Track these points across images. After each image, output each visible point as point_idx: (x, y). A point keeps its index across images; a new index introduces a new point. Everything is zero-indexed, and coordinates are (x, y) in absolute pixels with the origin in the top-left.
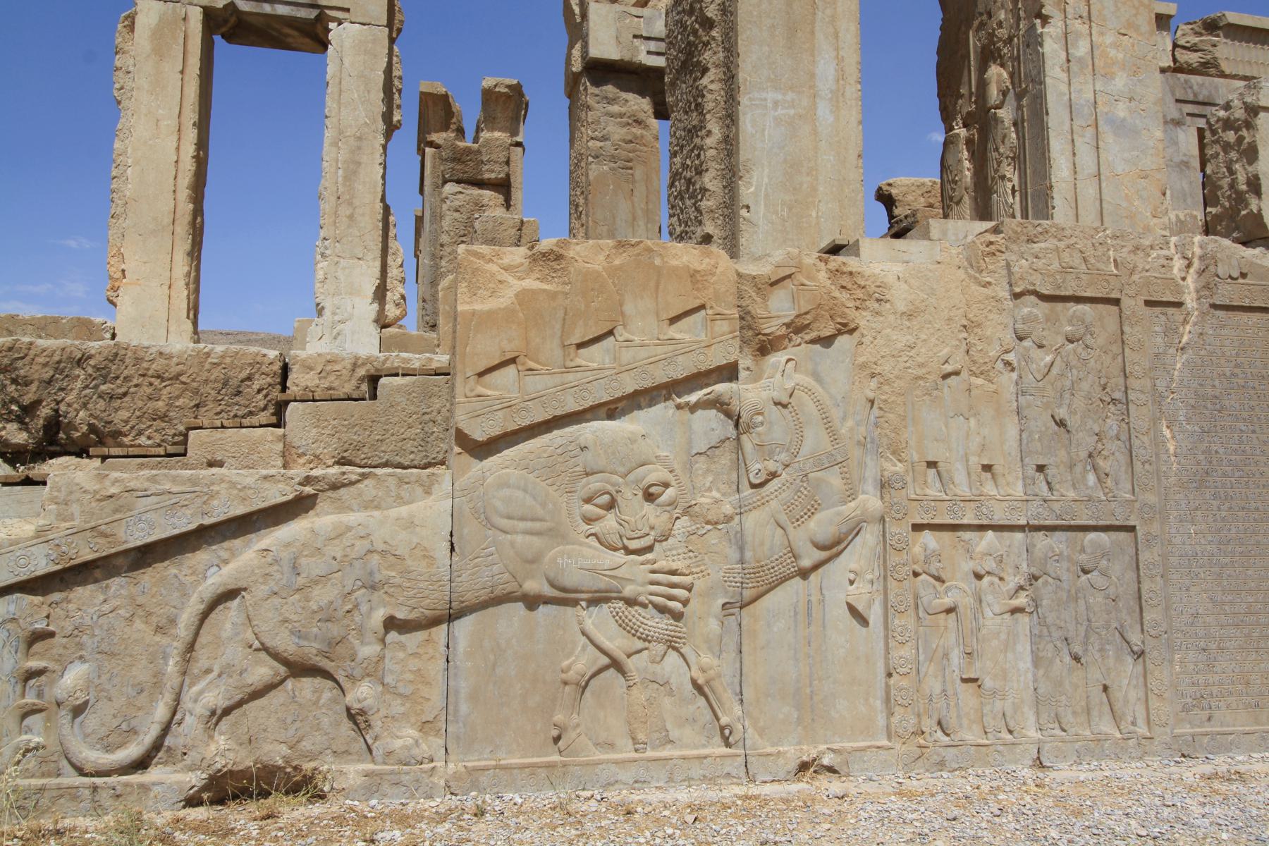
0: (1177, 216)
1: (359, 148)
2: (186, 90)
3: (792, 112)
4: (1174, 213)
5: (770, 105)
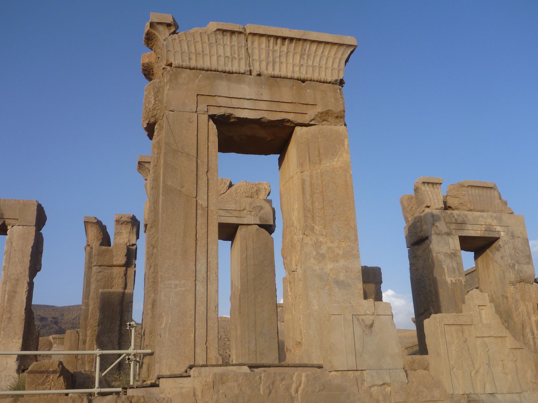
0: (451, 281)
3: (183, 289)
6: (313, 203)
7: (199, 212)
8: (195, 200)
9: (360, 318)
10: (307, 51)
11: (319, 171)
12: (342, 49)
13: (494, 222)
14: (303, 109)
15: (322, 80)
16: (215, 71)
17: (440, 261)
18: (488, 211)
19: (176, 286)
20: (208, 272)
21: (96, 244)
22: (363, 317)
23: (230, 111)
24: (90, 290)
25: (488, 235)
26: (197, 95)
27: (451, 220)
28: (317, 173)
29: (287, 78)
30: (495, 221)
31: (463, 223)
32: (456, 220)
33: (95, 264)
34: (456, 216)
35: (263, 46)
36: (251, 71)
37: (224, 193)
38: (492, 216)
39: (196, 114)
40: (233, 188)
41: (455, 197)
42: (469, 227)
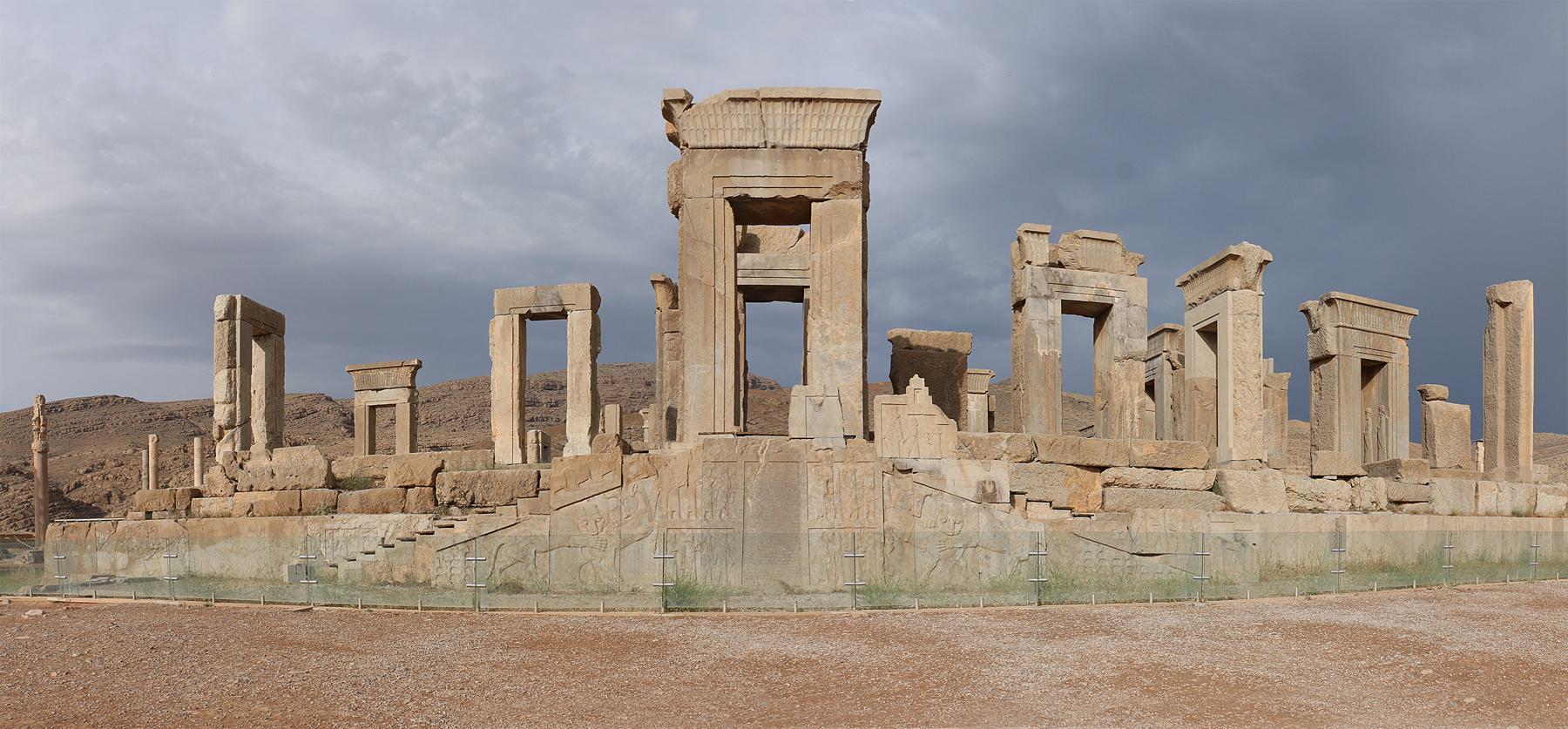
11: (829, 251)
16: (729, 148)
23: (745, 192)
28: (827, 253)
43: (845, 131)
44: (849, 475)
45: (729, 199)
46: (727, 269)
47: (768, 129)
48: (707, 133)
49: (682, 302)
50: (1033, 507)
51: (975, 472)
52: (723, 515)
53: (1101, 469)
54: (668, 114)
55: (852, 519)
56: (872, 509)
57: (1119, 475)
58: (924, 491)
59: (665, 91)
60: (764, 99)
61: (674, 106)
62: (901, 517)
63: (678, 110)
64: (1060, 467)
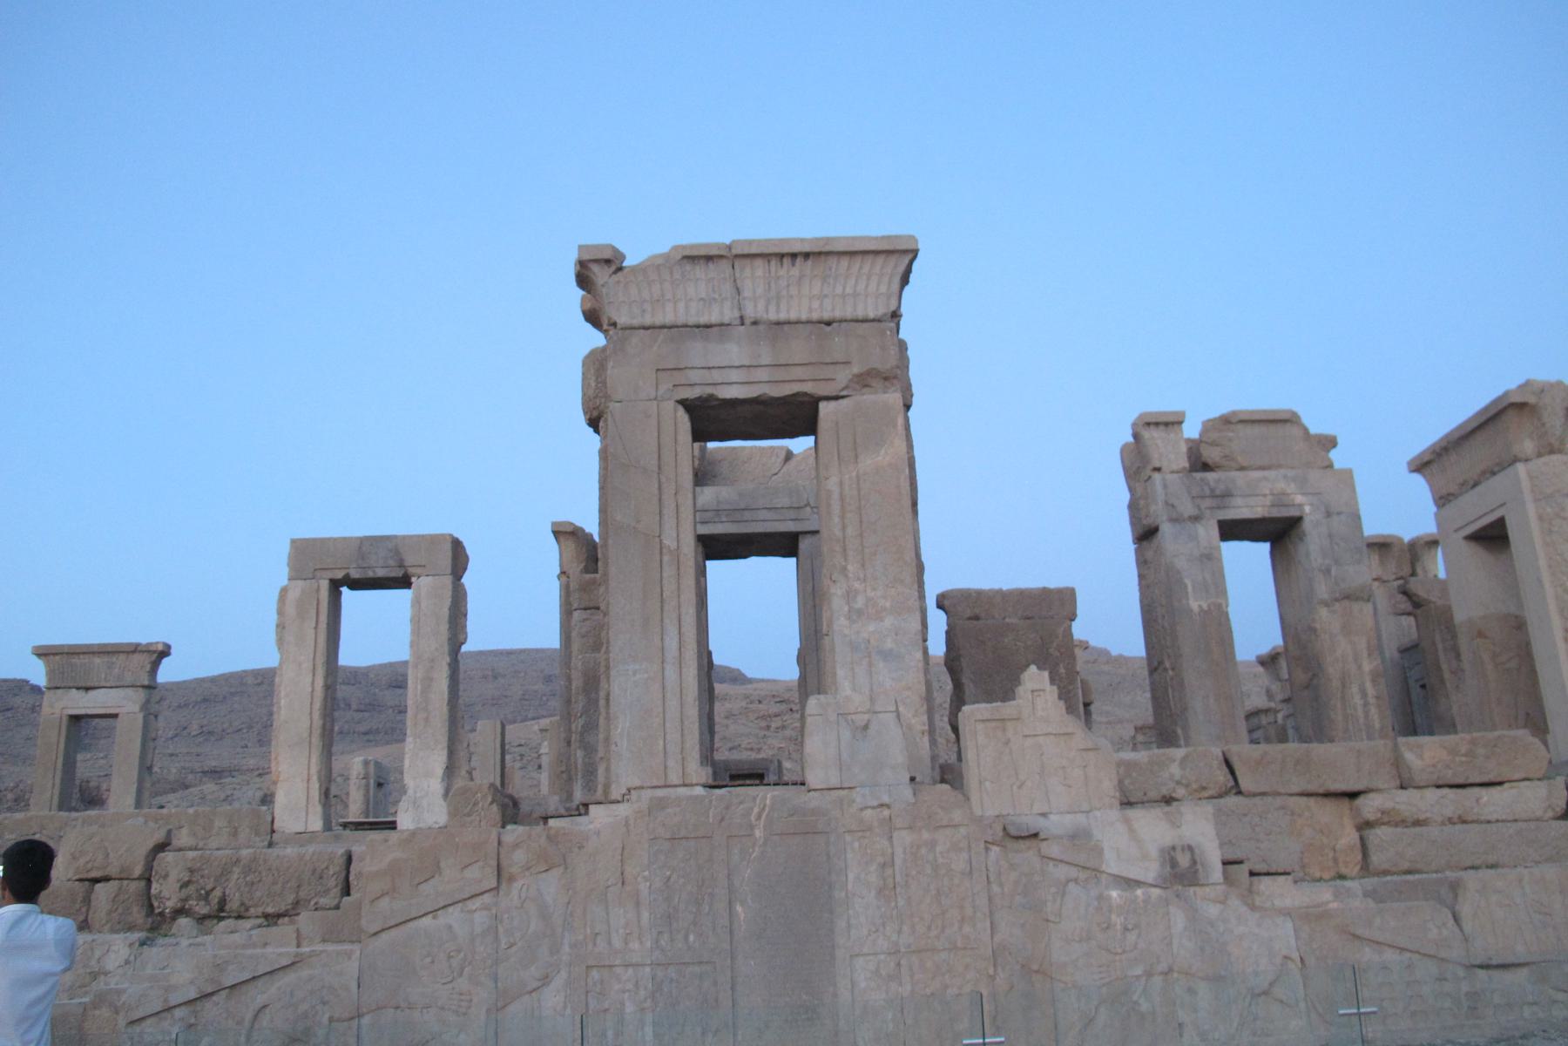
0: (1200, 606)
1: (432, 667)
2: (319, 641)
3: (646, 676)
4: (1197, 603)
5: (630, 673)
6: (844, 528)
7: (666, 558)
8: (657, 540)
9: (849, 717)
10: (833, 270)
11: (854, 474)
12: (893, 259)
13: (1291, 488)
14: (827, 372)
15: (860, 318)
17: (1179, 572)
18: (1279, 466)
19: (635, 673)
20: (682, 649)
21: (575, 569)
22: (853, 717)
23: (709, 390)
24: (571, 652)
25: (1276, 513)
26: (658, 370)
27: (1203, 490)
29: (802, 323)
30: (1293, 485)
31: (1227, 494)
32: (1212, 490)
33: (575, 606)
34: (1212, 484)
35: (759, 272)
36: (742, 318)
37: (776, 474)
38: (1285, 477)
39: (655, 402)
40: (792, 463)
41: (1214, 444)
42: (1239, 501)
43: (867, 296)
44: (923, 851)
45: (683, 402)
46: (682, 509)
47: (744, 299)
48: (647, 307)
49: (606, 564)
50: (1262, 887)
51: (1153, 828)
52: (691, 938)
53: (1353, 795)
54: (583, 280)
55: (934, 933)
56: (969, 911)
57: (1389, 805)
58: (1061, 872)
59: (581, 248)
60: (737, 256)
61: (595, 268)
62: (1023, 925)
63: (600, 275)
64: (1279, 801)
